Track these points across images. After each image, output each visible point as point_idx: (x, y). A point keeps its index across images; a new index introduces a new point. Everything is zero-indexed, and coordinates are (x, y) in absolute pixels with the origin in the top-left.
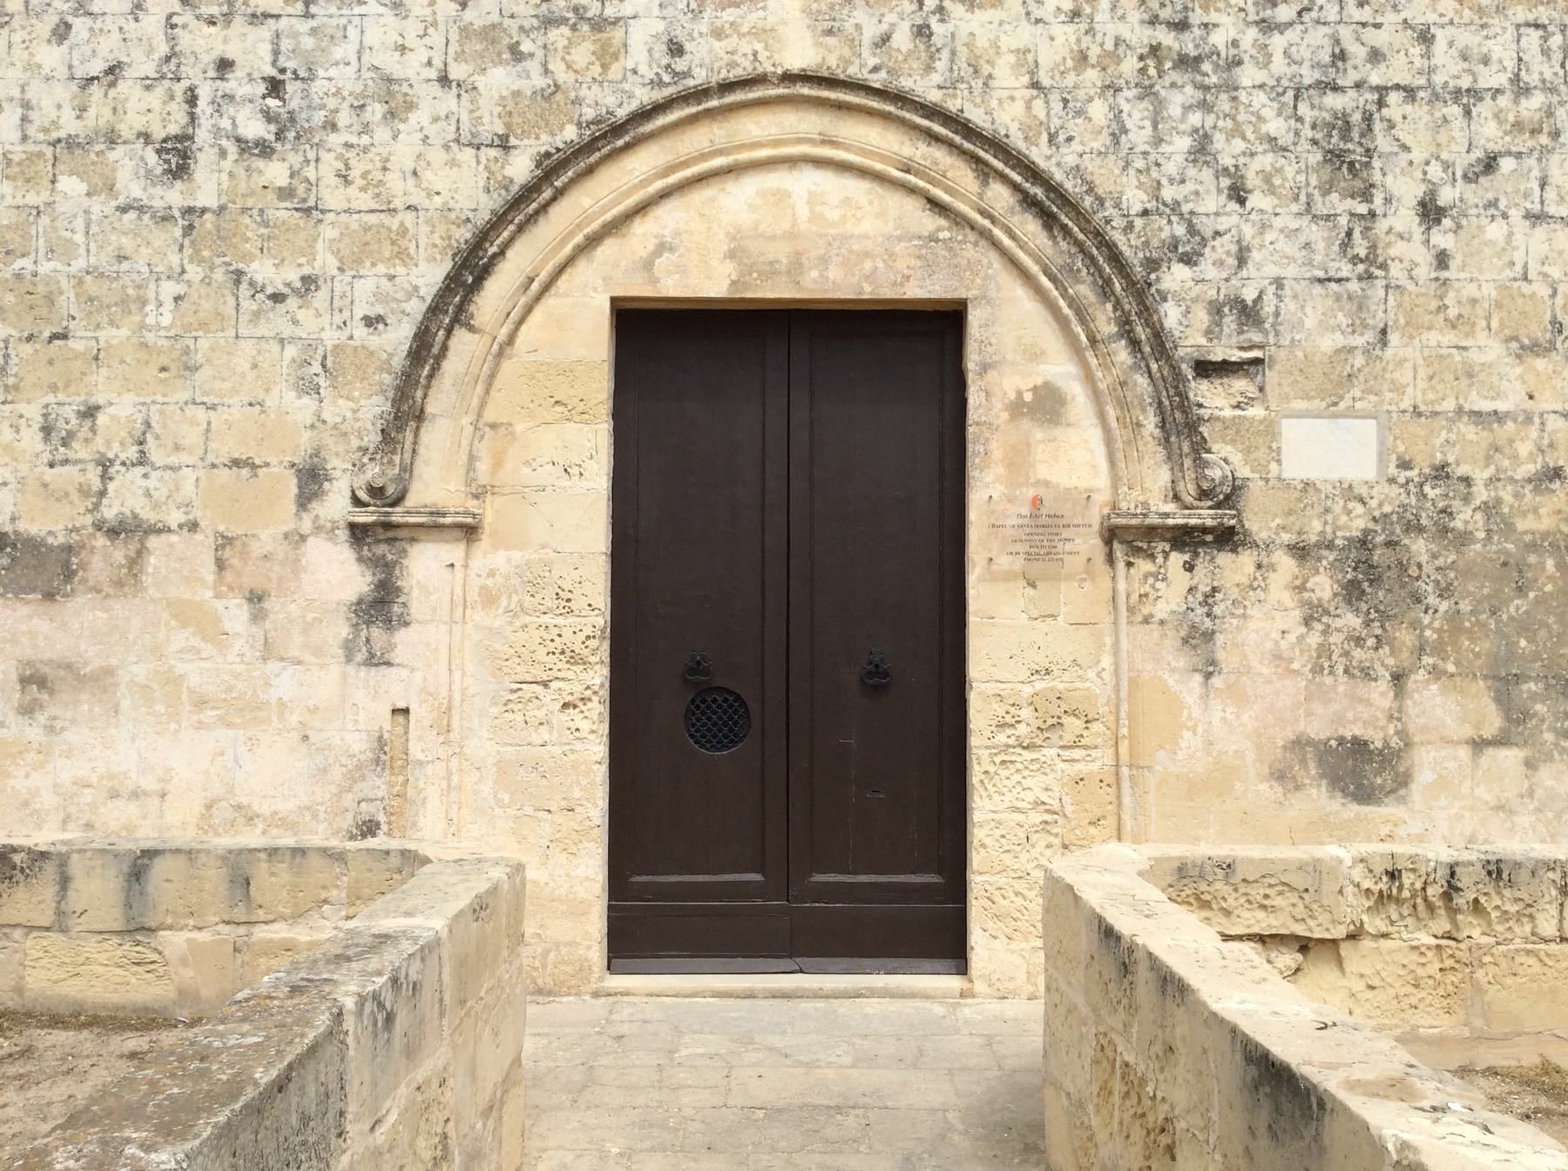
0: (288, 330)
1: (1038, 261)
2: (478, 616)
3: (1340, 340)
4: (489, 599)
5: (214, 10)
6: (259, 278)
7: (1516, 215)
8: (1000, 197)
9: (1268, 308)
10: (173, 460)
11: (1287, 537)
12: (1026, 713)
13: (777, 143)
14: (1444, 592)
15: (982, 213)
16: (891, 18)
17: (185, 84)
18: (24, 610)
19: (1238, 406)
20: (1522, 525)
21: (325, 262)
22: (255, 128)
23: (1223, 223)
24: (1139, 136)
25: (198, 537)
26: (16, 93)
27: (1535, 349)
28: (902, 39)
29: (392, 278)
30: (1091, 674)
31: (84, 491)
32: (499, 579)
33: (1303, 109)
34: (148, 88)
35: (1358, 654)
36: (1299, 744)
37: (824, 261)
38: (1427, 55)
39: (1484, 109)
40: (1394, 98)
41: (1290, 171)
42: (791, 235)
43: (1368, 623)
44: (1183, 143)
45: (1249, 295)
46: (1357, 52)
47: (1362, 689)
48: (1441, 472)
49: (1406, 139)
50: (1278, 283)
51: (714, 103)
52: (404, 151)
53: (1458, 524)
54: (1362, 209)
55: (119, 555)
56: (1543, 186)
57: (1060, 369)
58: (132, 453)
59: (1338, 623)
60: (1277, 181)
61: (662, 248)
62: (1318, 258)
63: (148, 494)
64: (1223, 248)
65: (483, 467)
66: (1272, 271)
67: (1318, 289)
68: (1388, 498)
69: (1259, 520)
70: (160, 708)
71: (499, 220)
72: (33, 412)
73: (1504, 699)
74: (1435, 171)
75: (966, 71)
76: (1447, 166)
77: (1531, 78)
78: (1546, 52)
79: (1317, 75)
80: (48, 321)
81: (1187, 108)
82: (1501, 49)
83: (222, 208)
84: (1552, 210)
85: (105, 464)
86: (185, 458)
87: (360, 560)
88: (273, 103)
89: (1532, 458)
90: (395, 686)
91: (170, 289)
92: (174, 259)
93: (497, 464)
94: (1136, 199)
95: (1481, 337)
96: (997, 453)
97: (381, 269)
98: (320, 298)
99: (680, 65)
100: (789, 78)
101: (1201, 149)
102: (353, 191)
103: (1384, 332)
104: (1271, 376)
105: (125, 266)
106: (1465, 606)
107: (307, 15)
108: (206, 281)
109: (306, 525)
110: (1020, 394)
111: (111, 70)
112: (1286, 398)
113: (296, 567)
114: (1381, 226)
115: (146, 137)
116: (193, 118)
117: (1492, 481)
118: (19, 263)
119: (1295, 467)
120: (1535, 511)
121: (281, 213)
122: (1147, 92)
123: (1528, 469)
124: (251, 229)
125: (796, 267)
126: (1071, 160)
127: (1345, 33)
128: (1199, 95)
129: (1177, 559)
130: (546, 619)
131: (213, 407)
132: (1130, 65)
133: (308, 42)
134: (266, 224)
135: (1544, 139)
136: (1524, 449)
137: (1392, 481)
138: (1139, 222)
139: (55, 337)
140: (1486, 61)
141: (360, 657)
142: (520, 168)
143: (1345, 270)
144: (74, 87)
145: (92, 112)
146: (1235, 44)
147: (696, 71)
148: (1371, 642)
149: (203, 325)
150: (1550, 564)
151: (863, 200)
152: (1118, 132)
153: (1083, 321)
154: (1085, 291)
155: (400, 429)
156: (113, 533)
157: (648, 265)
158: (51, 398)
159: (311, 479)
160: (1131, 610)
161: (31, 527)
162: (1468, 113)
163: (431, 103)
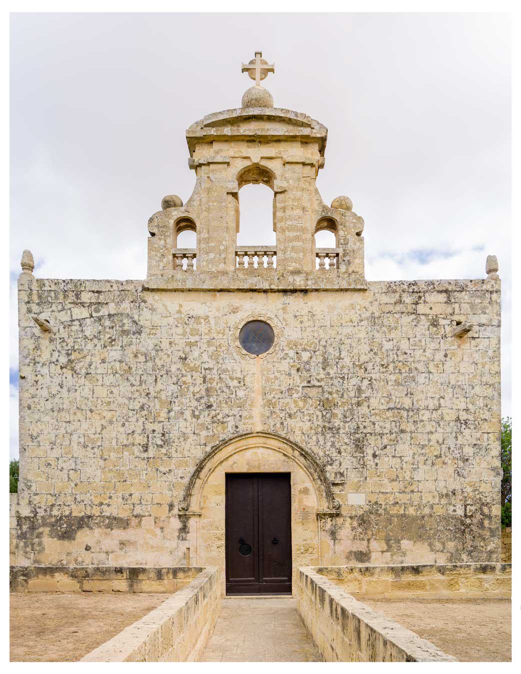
0: (167, 480)
1: (304, 465)
2: (202, 531)
3: (358, 479)
4: (203, 528)
5: (152, 421)
6: (161, 470)
7: (390, 456)
8: (297, 453)
9: (345, 474)
10: (146, 503)
11: (349, 515)
12: (302, 548)
13: (256, 444)
14: (377, 524)
15: (293, 456)
16: (276, 421)
17: (147, 434)
18: (120, 531)
19: (340, 491)
20: (391, 512)
21: (173, 467)
22: (160, 442)
23: (337, 458)
24: (322, 442)
25: (151, 517)
26: (115, 436)
27: (393, 480)
28: (278, 425)
29: (185, 470)
30: (314, 540)
31: (130, 509)
32: (205, 524)
33: (351, 437)
34: (140, 435)
35: (361, 536)
36: (351, 552)
37: (264, 465)
38: (374, 427)
39: (385, 437)
40: (368, 435)
41: (349, 449)
42: (258, 460)
43: (363, 530)
44: (330, 444)
45: (342, 471)
46: (362, 427)
47: (362, 542)
48: (376, 503)
49: (370, 443)
50: (347, 469)
51: (244, 437)
52: (187, 447)
53: (379, 512)
54: (362, 455)
55: (137, 521)
56: (395, 451)
57: (309, 484)
58: (139, 502)
59: (358, 530)
60: (347, 450)
61: (235, 463)
62: (354, 465)
63: (142, 510)
64: (337, 463)
65: (202, 504)
66: (346, 467)
67: (354, 470)
68: (367, 508)
69: (344, 511)
70: (145, 548)
71: (205, 459)
72: (120, 495)
73: (388, 544)
74: (375, 448)
75: (290, 431)
76: (377, 447)
77: (394, 431)
78: (396, 426)
79: (354, 431)
80: (123, 478)
81: (330, 437)
82: (388, 426)
83: (154, 457)
84: (397, 455)
85: (134, 504)
86: (148, 503)
87: (180, 521)
88: (163, 438)
89: (393, 500)
90: (187, 544)
91: (145, 472)
92: (145, 467)
93: (204, 503)
94: (321, 454)
95: (384, 478)
96: (297, 500)
97: (183, 468)
98: (172, 474)
99: (237, 430)
100: (258, 433)
101: (333, 445)
102: (178, 454)
103: (366, 478)
104: (345, 486)
105: (136, 468)
106: (380, 527)
107: (169, 422)
108: (152, 471)
109: (170, 515)
110: (301, 489)
111: (133, 432)
112: (348, 490)
113: (169, 523)
114: (366, 458)
115: (140, 444)
116: (148, 441)
117: (385, 505)
118: (117, 468)
119: (350, 502)
120: (393, 510)
121: (165, 458)
122: (323, 434)
123: (392, 502)
124: (160, 462)
125: (259, 466)
126: (309, 447)
127: (359, 423)
128: (333, 435)
129: (329, 519)
130: (215, 531)
131: (153, 494)
132: (320, 429)
133: (169, 427)
134: (162, 460)
135: (395, 442)
136: (391, 499)
137: (367, 505)
138: (322, 458)
139: (124, 481)
140: (385, 428)
141: (181, 539)
142: (208, 449)
143: (358, 466)
144: (126, 435)
145: (129, 440)
146: (339, 425)
147: (241, 431)
148: (364, 534)
149: (151, 479)
150: (396, 519)
151: (271, 454)
152: (318, 442)
153: (312, 476)
154: (312, 471)
155: (187, 497)
156: (136, 517)
157: (232, 466)
158: (123, 492)
159: (171, 506)
160: (321, 528)
161: (121, 516)
162: (381, 438)
163: (192, 437)
